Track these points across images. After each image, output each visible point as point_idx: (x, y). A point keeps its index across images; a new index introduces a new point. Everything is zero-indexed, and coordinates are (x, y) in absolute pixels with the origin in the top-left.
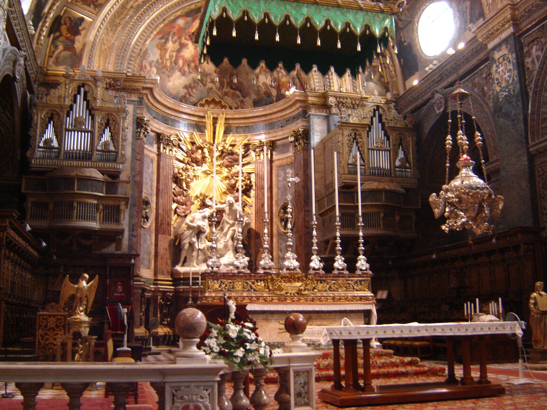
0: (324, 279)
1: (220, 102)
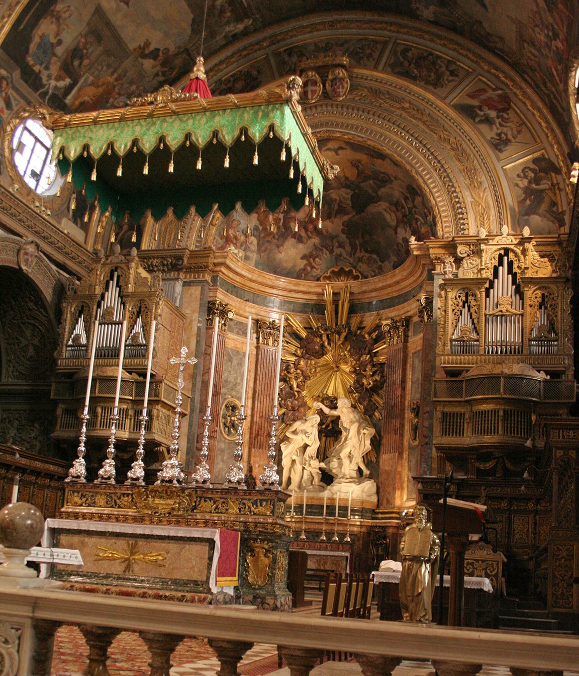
1: (351, 271)
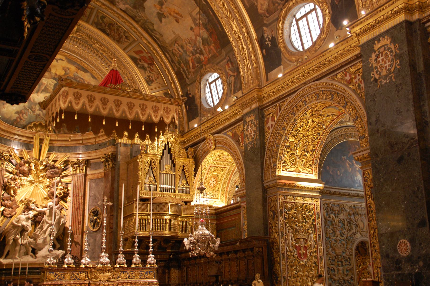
0: (125, 270)
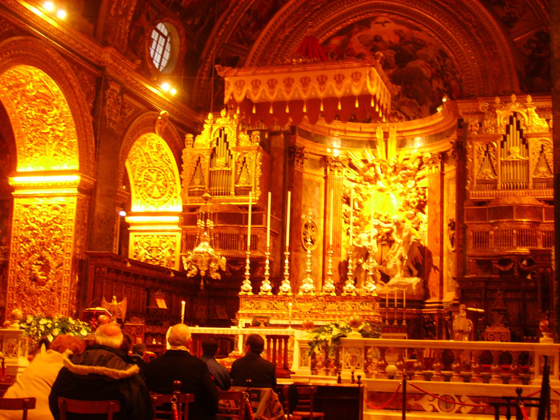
0: (333, 300)
